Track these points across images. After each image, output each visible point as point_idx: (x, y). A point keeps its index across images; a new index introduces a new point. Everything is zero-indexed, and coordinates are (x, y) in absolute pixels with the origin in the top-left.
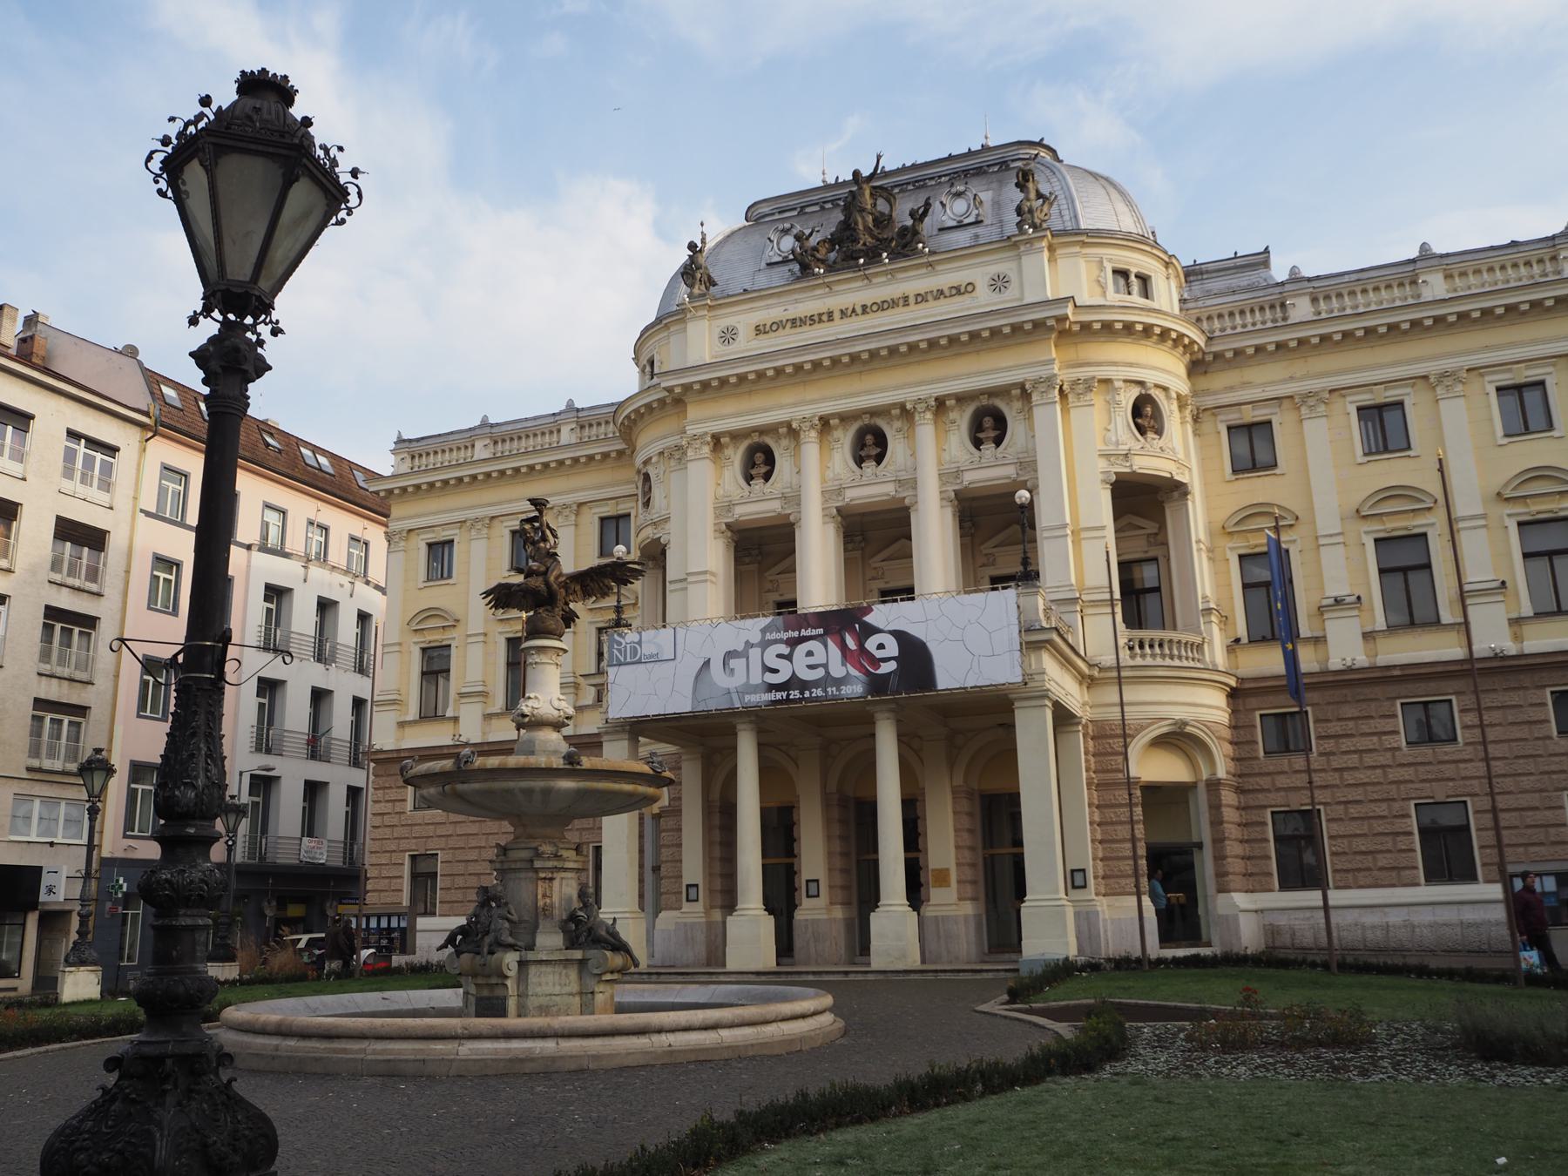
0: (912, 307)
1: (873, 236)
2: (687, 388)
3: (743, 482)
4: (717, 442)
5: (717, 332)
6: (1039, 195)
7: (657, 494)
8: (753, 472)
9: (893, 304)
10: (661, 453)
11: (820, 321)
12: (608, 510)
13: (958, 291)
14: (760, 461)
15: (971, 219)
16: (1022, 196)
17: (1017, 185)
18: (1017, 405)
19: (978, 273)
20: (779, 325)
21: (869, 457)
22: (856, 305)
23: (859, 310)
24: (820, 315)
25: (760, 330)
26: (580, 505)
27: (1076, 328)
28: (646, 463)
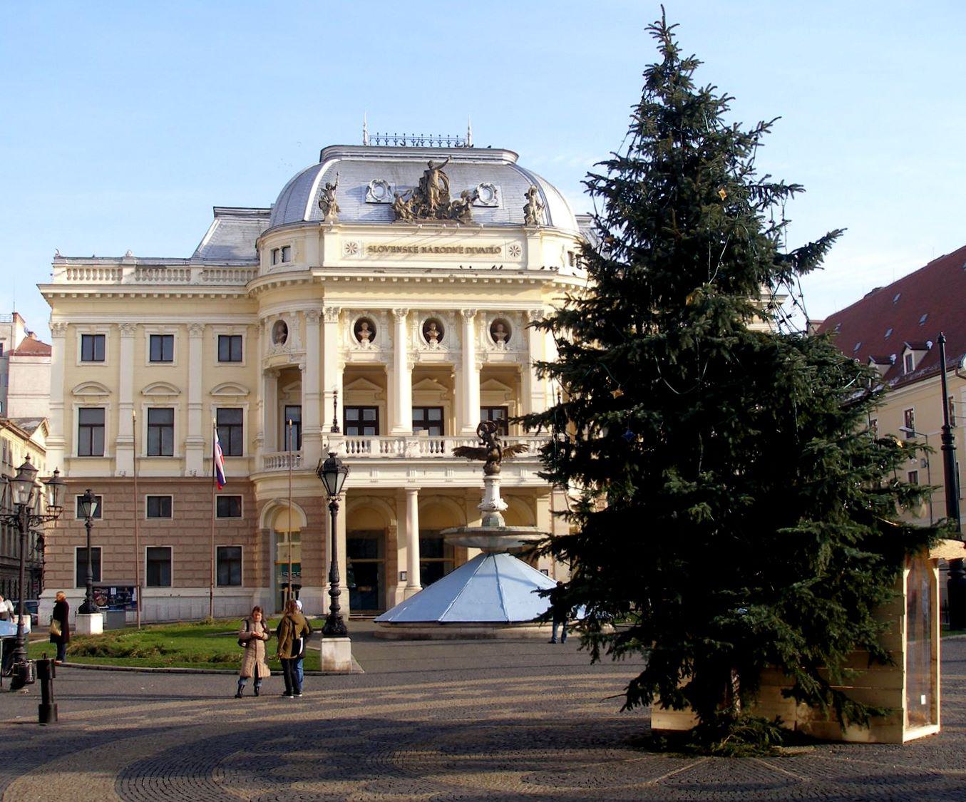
0: (464, 255)
1: (436, 202)
2: (327, 278)
3: (356, 341)
4: (341, 313)
5: (344, 246)
6: (537, 204)
7: (293, 335)
8: (360, 333)
9: (454, 250)
10: (298, 312)
11: (410, 251)
12: (226, 331)
13: (493, 250)
14: (365, 327)
15: (493, 204)
16: (528, 201)
17: (525, 195)
18: (518, 321)
19: (504, 242)
20: (385, 249)
21: (434, 336)
22: (432, 249)
23: (434, 250)
24: (410, 248)
25: (371, 249)
26: (207, 325)
27: (554, 285)
28: (281, 314)
